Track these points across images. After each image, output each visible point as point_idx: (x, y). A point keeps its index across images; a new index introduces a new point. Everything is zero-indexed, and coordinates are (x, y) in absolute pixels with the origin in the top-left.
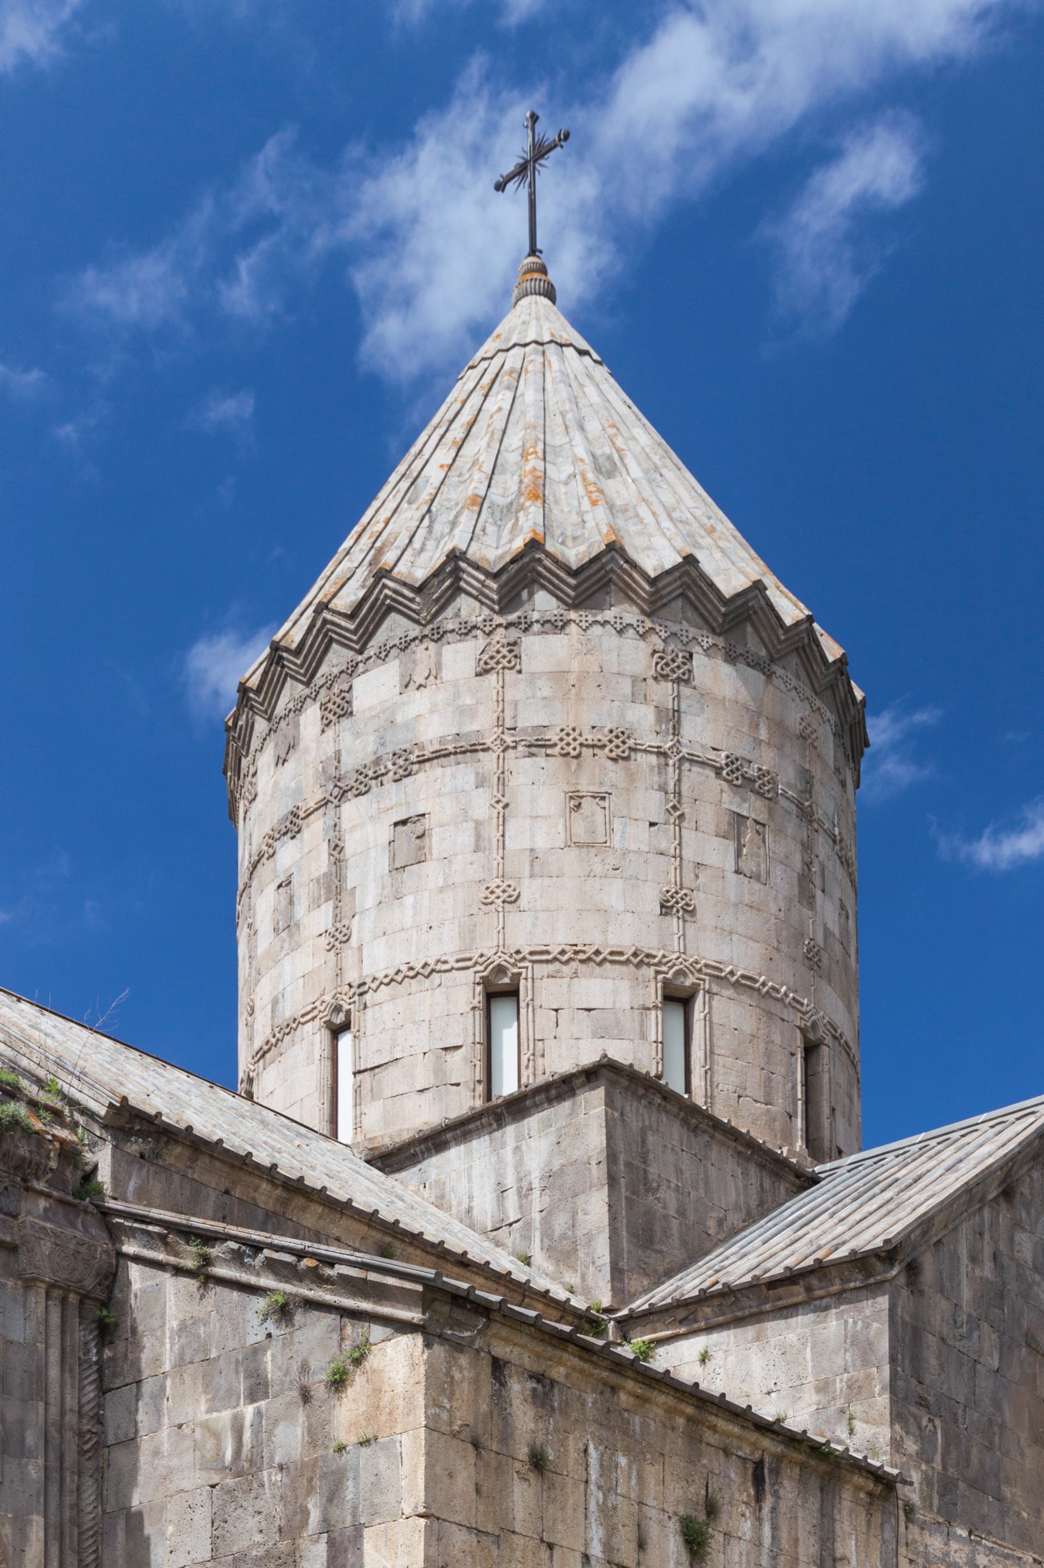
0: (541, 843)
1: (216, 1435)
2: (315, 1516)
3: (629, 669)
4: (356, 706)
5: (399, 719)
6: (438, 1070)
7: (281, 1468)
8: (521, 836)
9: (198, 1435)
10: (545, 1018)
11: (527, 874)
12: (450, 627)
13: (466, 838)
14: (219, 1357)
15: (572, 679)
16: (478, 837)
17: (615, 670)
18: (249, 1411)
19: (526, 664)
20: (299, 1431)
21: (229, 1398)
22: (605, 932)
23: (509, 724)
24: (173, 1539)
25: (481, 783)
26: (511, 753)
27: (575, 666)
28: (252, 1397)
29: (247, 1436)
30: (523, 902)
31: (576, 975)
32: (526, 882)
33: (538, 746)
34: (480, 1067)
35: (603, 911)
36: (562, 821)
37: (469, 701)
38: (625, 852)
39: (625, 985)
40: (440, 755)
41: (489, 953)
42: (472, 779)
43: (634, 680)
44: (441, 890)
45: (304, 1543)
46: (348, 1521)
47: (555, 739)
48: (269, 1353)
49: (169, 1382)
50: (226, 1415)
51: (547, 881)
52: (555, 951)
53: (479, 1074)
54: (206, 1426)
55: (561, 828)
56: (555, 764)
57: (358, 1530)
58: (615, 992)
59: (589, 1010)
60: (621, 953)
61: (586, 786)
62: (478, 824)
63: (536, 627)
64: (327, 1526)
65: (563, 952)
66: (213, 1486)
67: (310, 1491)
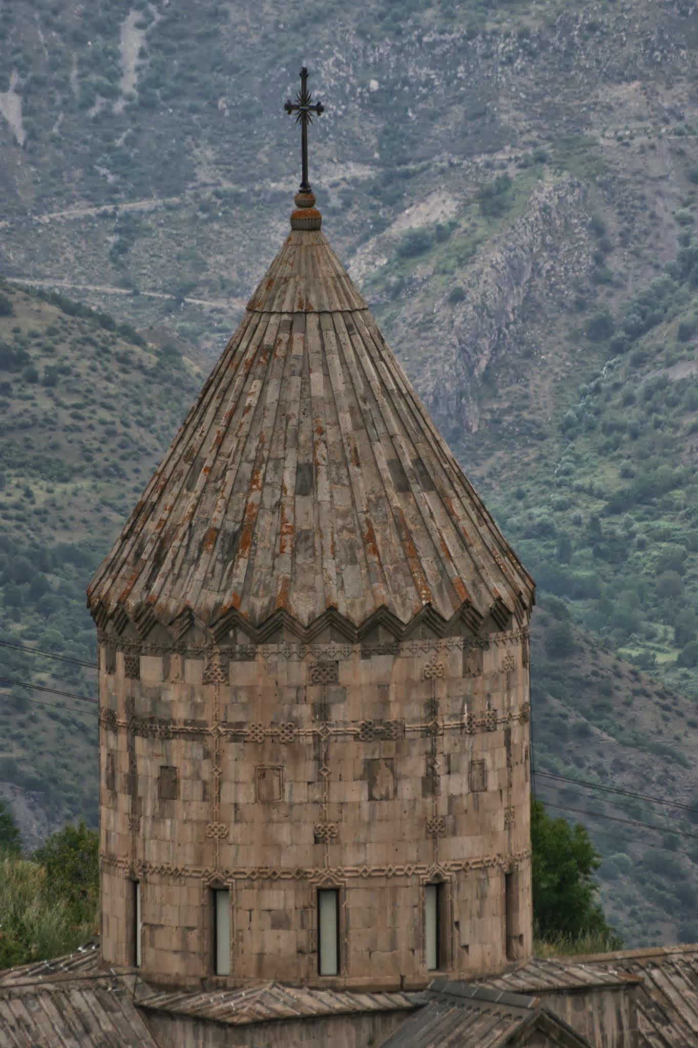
0: (241, 800)
3: (294, 681)
6: (184, 940)
8: (228, 795)
10: (244, 915)
11: (233, 819)
13: (197, 791)
16: (205, 792)
17: (286, 683)
22: (279, 859)
23: (222, 719)
25: (207, 755)
26: (224, 739)
27: (261, 682)
30: (231, 839)
31: (262, 888)
32: (232, 824)
34: (207, 943)
35: (278, 846)
36: (253, 786)
37: (199, 700)
38: (291, 806)
39: (291, 894)
41: (211, 870)
42: (201, 752)
43: (298, 689)
44: (185, 822)
47: (249, 732)
51: (244, 825)
52: (248, 872)
53: (207, 948)
55: (252, 790)
56: (249, 748)
58: (285, 898)
59: (270, 910)
60: (289, 873)
61: (268, 763)
62: (205, 783)
63: (238, 656)
65: (253, 873)
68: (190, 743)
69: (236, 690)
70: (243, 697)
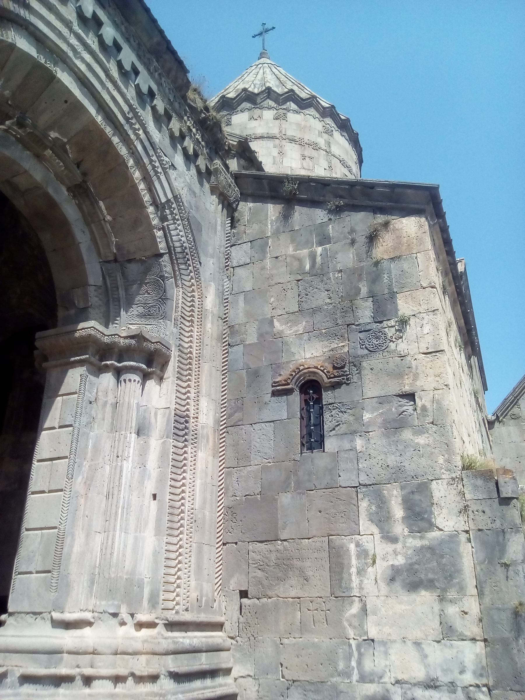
1: (300, 260)
2: (364, 290)
4: (232, 123)
5: (248, 127)
7: (341, 271)
9: (288, 260)
12: (265, 106)
14: (300, 229)
15: (302, 126)
18: (319, 250)
19: (288, 119)
20: (351, 256)
21: (308, 244)
24: (274, 303)
28: (320, 244)
29: (319, 259)
33: (292, 140)
37: (271, 125)
40: (262, 137)
45: (359, 302)
46: (386, 291)
48: (330, 226)
49: (270, 241)
50: (305, 252)
54: (293, 257)
57: (393, 295)
64: (372, 295)
66: (298, 281)
67: (360, 279)
68: (265, 142)
69: (291, 123)
70: (294, 127)
